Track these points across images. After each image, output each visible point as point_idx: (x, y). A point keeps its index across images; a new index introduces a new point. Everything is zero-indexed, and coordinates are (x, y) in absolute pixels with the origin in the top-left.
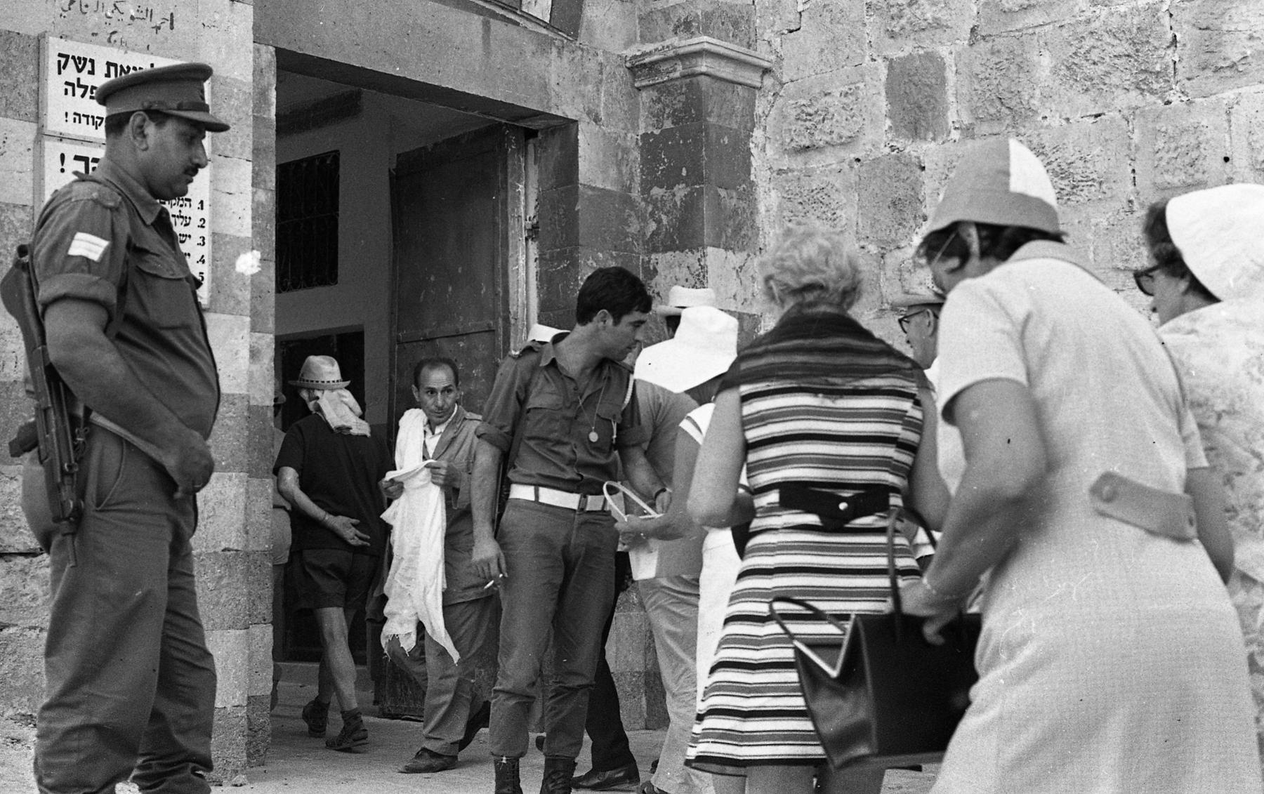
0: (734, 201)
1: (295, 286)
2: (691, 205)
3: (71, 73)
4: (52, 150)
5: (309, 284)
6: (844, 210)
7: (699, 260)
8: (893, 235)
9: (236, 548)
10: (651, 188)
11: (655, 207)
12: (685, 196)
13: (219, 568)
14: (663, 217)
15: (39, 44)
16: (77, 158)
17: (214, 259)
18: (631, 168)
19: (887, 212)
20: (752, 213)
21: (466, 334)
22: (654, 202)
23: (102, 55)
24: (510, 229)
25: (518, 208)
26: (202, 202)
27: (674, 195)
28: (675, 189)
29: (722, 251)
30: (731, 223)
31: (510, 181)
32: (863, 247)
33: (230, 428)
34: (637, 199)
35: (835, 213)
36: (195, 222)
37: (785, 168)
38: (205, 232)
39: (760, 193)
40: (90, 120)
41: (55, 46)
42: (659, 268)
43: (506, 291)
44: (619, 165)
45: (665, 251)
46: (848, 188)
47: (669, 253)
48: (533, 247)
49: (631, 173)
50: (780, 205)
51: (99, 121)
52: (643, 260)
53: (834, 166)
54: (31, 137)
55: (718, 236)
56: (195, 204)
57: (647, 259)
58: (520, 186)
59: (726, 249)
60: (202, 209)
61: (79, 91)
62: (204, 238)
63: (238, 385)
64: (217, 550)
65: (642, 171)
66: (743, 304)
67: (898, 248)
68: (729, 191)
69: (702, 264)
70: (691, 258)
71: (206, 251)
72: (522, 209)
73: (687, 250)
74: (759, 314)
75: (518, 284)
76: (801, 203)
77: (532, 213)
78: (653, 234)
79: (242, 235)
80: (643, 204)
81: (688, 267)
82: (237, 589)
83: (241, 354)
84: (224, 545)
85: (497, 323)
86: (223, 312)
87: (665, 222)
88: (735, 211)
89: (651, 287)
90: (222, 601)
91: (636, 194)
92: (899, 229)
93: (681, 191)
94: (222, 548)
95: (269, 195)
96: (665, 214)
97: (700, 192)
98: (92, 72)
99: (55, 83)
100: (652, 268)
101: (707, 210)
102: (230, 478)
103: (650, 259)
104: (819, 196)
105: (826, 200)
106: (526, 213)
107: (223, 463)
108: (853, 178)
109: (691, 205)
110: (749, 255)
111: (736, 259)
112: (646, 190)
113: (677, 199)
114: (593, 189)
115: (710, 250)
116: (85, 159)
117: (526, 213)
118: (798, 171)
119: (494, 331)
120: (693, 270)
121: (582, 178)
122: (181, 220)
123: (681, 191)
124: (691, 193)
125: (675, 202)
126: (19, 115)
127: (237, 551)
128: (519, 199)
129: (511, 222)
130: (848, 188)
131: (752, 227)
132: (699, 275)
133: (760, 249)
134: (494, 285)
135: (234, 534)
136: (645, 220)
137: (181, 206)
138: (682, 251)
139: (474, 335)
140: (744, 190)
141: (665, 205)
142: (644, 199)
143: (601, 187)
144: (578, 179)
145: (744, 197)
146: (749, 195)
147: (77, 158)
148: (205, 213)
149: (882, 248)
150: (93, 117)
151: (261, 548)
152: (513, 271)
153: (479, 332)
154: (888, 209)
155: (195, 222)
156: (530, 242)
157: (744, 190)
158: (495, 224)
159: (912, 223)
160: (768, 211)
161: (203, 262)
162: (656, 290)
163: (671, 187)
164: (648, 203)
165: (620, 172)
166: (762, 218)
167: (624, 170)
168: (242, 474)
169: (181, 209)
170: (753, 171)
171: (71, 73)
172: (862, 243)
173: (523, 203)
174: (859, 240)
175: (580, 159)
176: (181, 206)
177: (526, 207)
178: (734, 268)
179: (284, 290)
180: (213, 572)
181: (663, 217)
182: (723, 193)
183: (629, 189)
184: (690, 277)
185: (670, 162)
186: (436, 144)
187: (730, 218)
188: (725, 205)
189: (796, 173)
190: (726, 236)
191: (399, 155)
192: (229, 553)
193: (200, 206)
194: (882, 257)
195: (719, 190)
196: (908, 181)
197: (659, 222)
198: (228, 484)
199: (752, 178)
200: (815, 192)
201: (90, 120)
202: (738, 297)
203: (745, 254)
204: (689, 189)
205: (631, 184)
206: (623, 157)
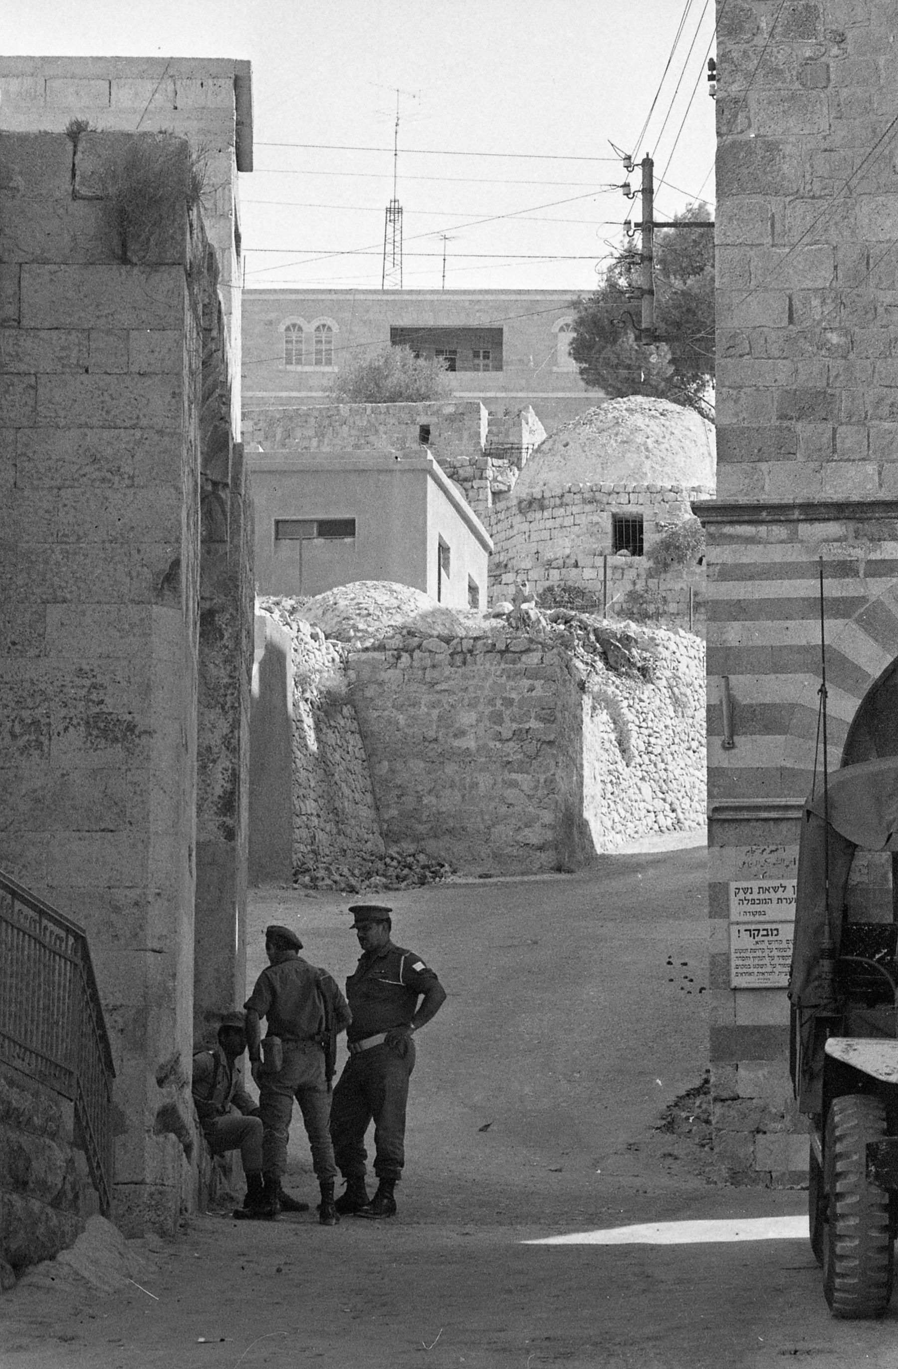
3: (741, 895)
4: (735, 929)
15: (728, 884)
16: (746, 930)
23: (755, 884)
41: (733, 886)
54: (726, 924)
61: (746, 902)
98: (751, 893)
99: (734, 901)
116: (750, 931)
126: (720, 917)
147: (746, 930)
171: (741, 895)
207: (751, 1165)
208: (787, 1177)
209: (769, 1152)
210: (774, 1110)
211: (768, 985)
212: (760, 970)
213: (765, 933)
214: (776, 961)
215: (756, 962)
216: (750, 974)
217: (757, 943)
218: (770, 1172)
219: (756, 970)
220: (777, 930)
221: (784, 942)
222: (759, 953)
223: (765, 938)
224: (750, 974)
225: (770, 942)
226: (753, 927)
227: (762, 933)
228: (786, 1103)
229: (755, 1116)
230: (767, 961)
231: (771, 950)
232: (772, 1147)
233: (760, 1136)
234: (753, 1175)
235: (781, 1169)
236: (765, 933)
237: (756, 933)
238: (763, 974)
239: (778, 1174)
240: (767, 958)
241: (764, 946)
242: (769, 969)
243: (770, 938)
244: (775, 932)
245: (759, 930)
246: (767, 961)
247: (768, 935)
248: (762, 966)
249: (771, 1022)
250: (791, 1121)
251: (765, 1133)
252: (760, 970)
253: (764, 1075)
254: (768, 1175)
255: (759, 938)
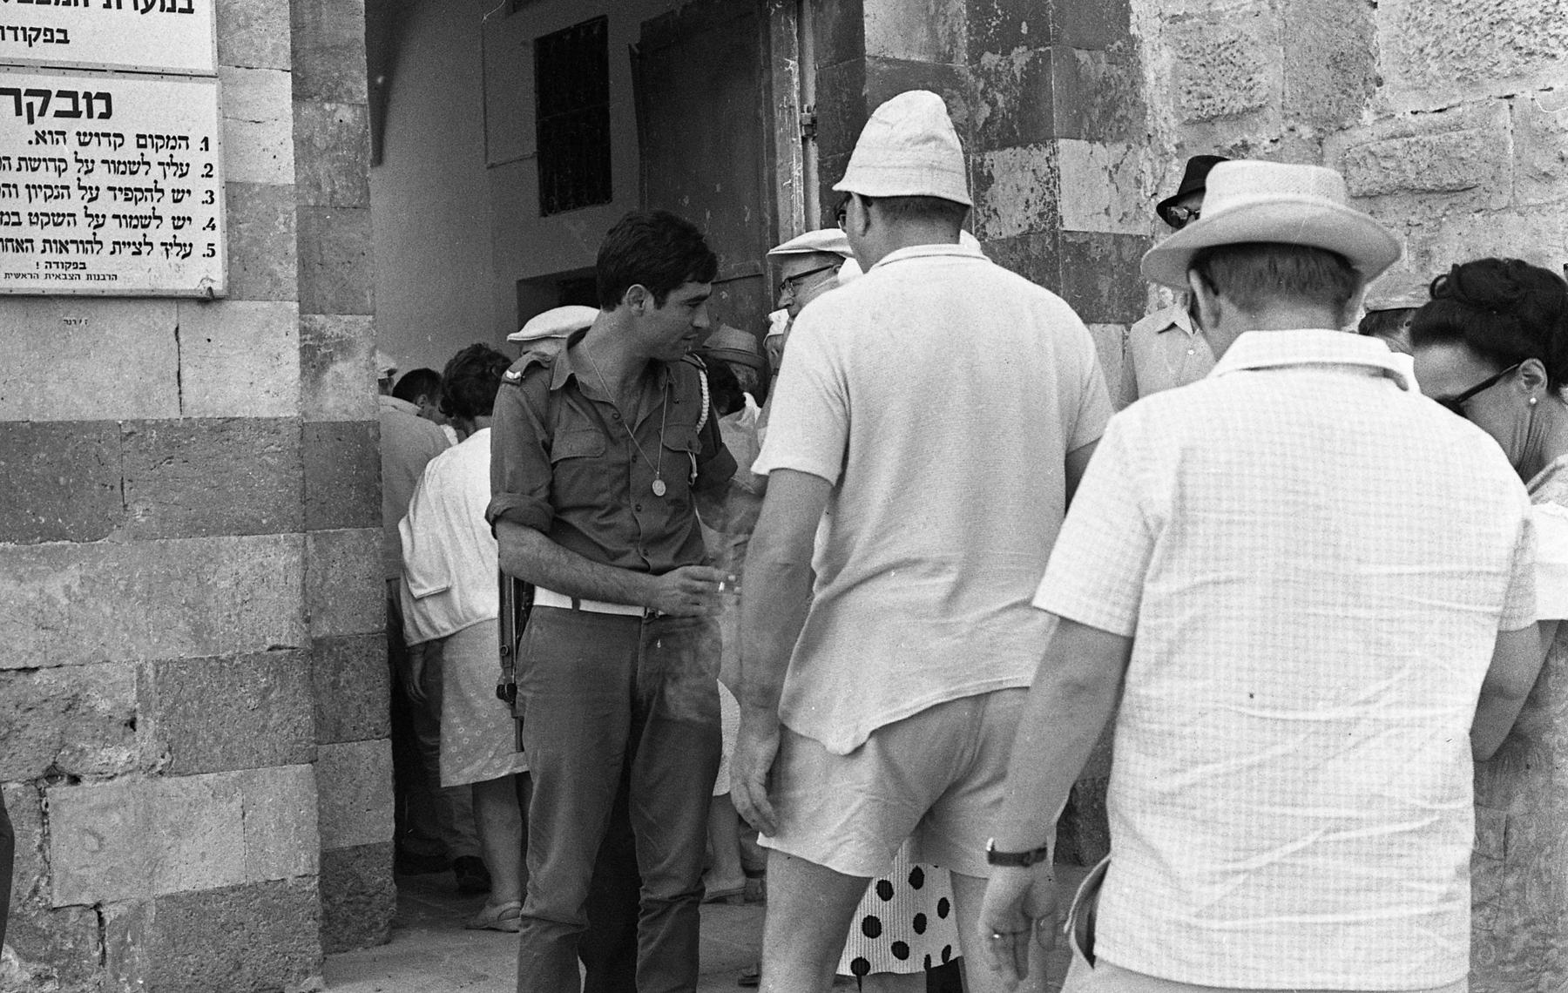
0: (1104, 66)
1: (564, 207)
2: (1034, 77)
5: (580, 204)
6: (1265, 73)
7: (1048, 160)
8: (1334, 110)
9: (290, 645)
10: (981, 54)
11: (989, 83)
12: (1027, 64)
13: (266, 674)
14: (1000, 97)
17: (231, 224)
18: (952, 26)
19: (1323, 73)
20: (1133, 84)
21: (729, 281)
22: (986, 74)
24: (776, 126)
25: (789, 96)
26: (206, 140)
27: (1012, 64)
28: (1013, 54)
29: (1083, 143)
30: (1099, 99)
31: (774, 56)
32: (1292, 130)
33: (271, 469)
34: (962, 72)
35: (1250, 80)
36: (197, 170)
37: (1181, 13)
38: (215, 184)
39: (1146, 52)
40: (20, 33)
42: (994, 174)
43: (775, 217)
44: (931, 22)
45: (1003, 147)
46: (1271, 38)
47: (1009, 150)
48: (813, 149)
49: (952, 34)
50: (1175, 70)
51: (34, 34)
52: (974, 160)
53: (1248, 8)
55: (1078, 121)
56: (196, 143)
57: (979, 160)
58: (792, 62)
59: (1091, 140)
60: (207, 149)
62: (212, 193)
63: (283, 404)
64: (259, 649)
65: (969, 29)
66: (1120, 221)
67: (1341, 128)
68: (1093, 53)
69: (1052, 165)
70: (1037, 157)
71: (217, 211)
72: (795, 96)
73: (1032, 145)
74: (1149, 235)
75: (791, 206)
76: (1204, 65)
77: (811, 101)
78: (987, 122)
79: (281, 182)
80: (972, 78)
81: (1034, 171)
82: (296, 704)
83: (284, 358)
84: (270, 641)
85: (765, 265)
86: (253, 298)
87: (1001, 104)
88: (1105, 83)
89: (986, 201)
90: (271, 723)
91: (960, 64)
92: (1342, 100)
93: (1020, 56)
94: (267, 647)
95: (358, 112)
96: (1001, 92)
97: (1047, 55)
100: (985, 171)
101: (1054, 82)
102: (276, 542)
103: (983, 160)
104: (1227, 54)
105: (1238, 60)
106: (803, 100)
107: (264, 521)
108: (1276, 24)
109: (1034, 77)
110: (1129, 147)
111: (1105, 154)
112: (975, 58)
113: (1016, 70)
114: (888, 61)
115: (1062, 143)
116: (16, 93)
117: (803, 100)
118: (1199, 16)
119: (762, 275)
120: (1040, 174)
121: (870, 48)
122: (173, 168)
123: (1020, 56)
124: (1034, 60)
125: (1014, 75)
127: (293, 648)
128: (789, 81)
129: (778, 115)
130: (1271, 38)
131: (1134, 104)
132: (1048, 183)
133: (1149, 136)
134: (758, 208)
135: (286, 624)
136: (975, 103)
137: (173, 148)
138: (1025, 147)
139: (737, 282)
140: (1119, 49)
141: (1001, 80)
142: (973, 72)
143: (903, 58)
144: (864, 50)
145: (1119, 60)
146: (1128, 55)
148: (213, 156)
149: (1320, 130)
150: (24, 29)
151: (364, 630)
152: (783, 188)
153: (744, 278)
154: (1325, 70)
155: (197, 170)
156: (810, 142)
157: (1119, 49)
158: (758, 119)
159: (1361, 90)
160: (1158, 79)
161: (213, 228)
162: (992, 207)
163: (1006, 53)
164: (978, 77)
165: (933, 33)
166: (1151, 91)
167: (940, 29)
168: (294, 535)
169: (172, 152)
170: (1133, 18)
172: (1291, 123)
173: (797, 88)
174: (1285, 117)
175: (866, 20)
176: (173, 148)
177: (802, 92)
178: (1106, 168)
179: (550, 212)
180: (255, 682)
181: (1000, 97)
182: (1083, 56)
183: (950, 58)
184: (1036, 185)
185: (1005, 15)
186: (685, 7)
187: (1097, 92)
188: (1088, 77)
189: (1196, 20)
190: (1091, 121)
191: (643, 25)
192: (279, 653)
193: (203, 146)
194: (1320, 144)
195: (1076, 52)
196: (1353, 26)
197: (993, 103)
198: (271, 550)
199: (1133, 30)
200: (1222, 48)
201: (20, 33)
202: (1111, 211)
203: (1122, 147)
204: (1032, 54)
205: (951, 50)
206: (937, 11)
207: (35, 891)
208: (151, 912)
209: (92, 843)
210: (104, 706)
211: (82, 286)
212: (52, 233)
213: (66, 104)
214: (107, 205)
215: (39, 205)
216: (20, 245)
217: (41, 137)
218: (97, 906)
219: (37, 234)
220: (106, 97)
221: (131, 141)
222: (46, 176)
223: (72, 126)
224: (20, 245)
225: (84, 139)
226: (23, 82)
227: (57, 104)
228: (140, 675)
229: (42, 729)
230: (74, 203)
231: (88, 166)
232: (101, 826)
233: (59, 792)
234: (43, 924)
235: (132, 892)
236: (66, 104)
237: (38, 102)
238: (63, 246)
239: (121, 909)
240: (76, 193)
241: (66, 150)
242: (83, 231)
243: (84, 124)
244: (99, 106)
245: (46, 94)
246: (74, 203)
247: (76, 113)
248: (57, 219)
249: (89, 412)
250: (160, 736)
251: (75, 780)
252: (52, 233)
253: (67, 588)
254: (94, 915)
255: (43, 124)
